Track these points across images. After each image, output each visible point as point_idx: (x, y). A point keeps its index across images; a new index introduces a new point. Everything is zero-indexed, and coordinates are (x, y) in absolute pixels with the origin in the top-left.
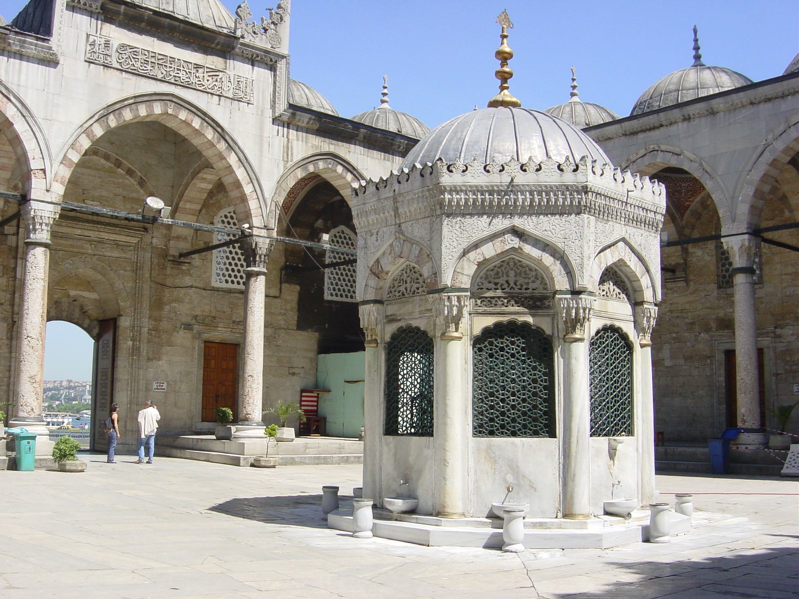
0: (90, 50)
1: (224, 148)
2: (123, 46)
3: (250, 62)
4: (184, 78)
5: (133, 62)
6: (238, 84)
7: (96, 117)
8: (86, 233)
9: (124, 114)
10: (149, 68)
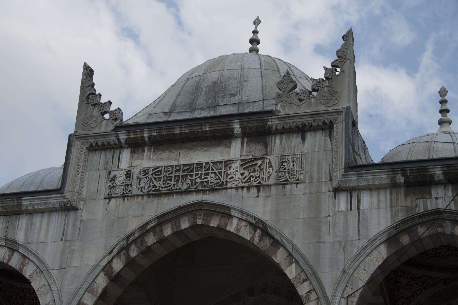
0: (110, 186)
1: (268, 245)
2: (145, 172)
3: (300, 135)
4: (212, 181)
5: (155, 182)
6: (282, 165)
7: (115, 252)
9: (146, 240)
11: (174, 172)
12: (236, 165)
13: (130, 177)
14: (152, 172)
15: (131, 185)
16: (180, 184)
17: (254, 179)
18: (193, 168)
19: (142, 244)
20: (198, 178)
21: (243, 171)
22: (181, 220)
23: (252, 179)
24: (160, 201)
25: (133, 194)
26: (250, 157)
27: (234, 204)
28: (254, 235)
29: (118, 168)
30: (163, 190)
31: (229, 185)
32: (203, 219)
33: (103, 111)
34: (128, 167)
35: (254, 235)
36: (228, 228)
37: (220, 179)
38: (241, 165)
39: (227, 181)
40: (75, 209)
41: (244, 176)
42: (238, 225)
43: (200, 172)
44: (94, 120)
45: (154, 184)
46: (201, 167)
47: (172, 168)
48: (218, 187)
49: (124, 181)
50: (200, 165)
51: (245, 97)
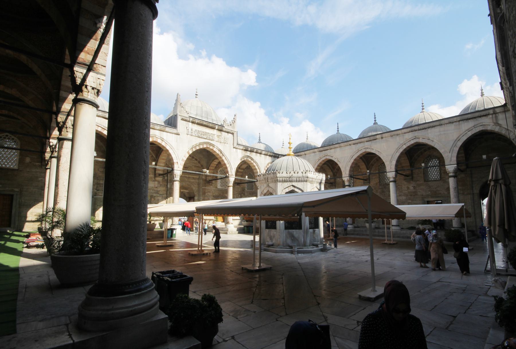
7: (190, 149)
8: (186, 175)
10: (202, 135)
12: (216, 136)
30: (201, 137)
40: (179, 135)
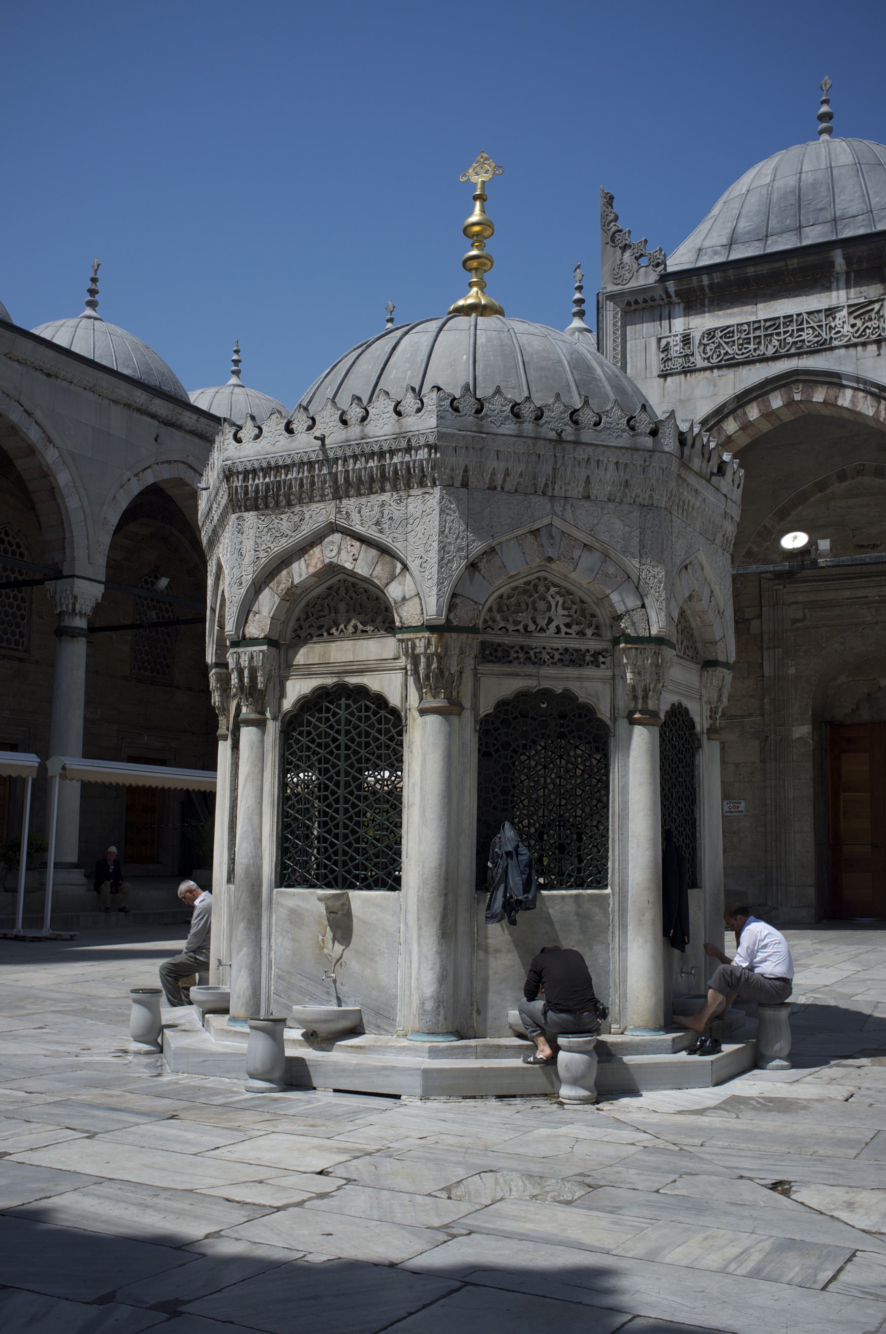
0: (663, 359)
2: (710, 334)
4: (809, 339)
5: (727, 348)
9: (725, 428)
11: (752, 332)
13: (689, 343)
14: (720, 335)
15: (692, 355)
16: (762, 348)
17: (871, 331)
18: (780, 324)
19: (719, 434)
20: (789, 336)
21: (853, 321)
22: (771, 396)
23: (868, 331)
24: (737, 373)
25: (697, 367)
26: (862, 300)
27: (847, 368)
28: (878, 408)
29: (670, 332)
31: (835, 343)
32: (802, 393)
33: (637, 255)
34: (684, 330)
35: (878, 408)
36: (840, 403)
37: (821, 336)
38: (850, 313)
39: (831, 338)
41: (856, 328)
42: (853, 396)
43: (790, 328)
44: (626, 269)
45: (725, 351)
46: (792, 321)
47: (749, 326)
48: (819, 348)
49: (682, 350)
50: (789, 318)
51: (841, 211)
